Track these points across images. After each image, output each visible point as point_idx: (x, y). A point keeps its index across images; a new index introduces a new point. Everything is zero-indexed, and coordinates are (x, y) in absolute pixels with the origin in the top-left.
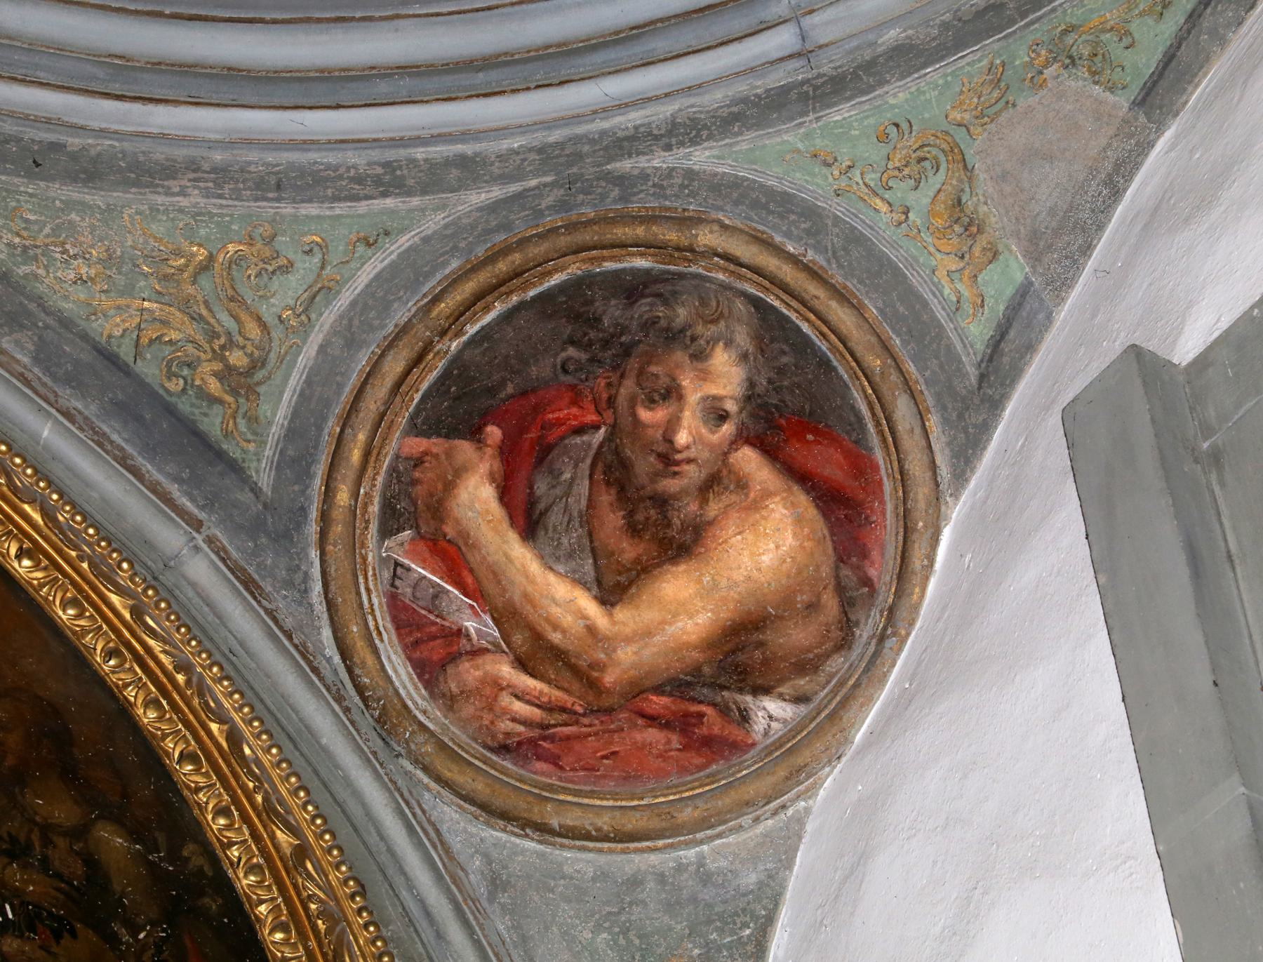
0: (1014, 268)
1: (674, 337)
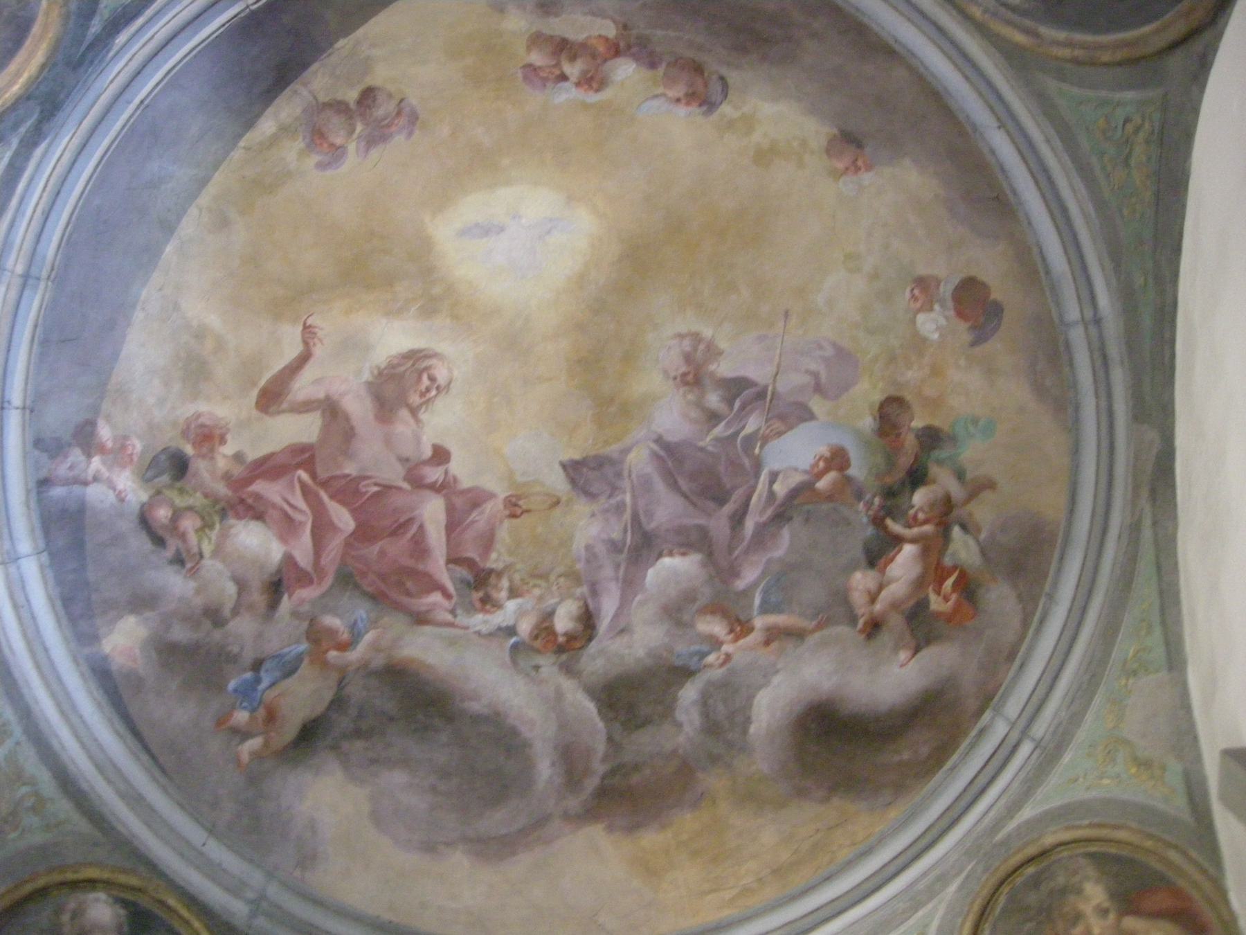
0: (1175, 768)
1: (1063, 892)
